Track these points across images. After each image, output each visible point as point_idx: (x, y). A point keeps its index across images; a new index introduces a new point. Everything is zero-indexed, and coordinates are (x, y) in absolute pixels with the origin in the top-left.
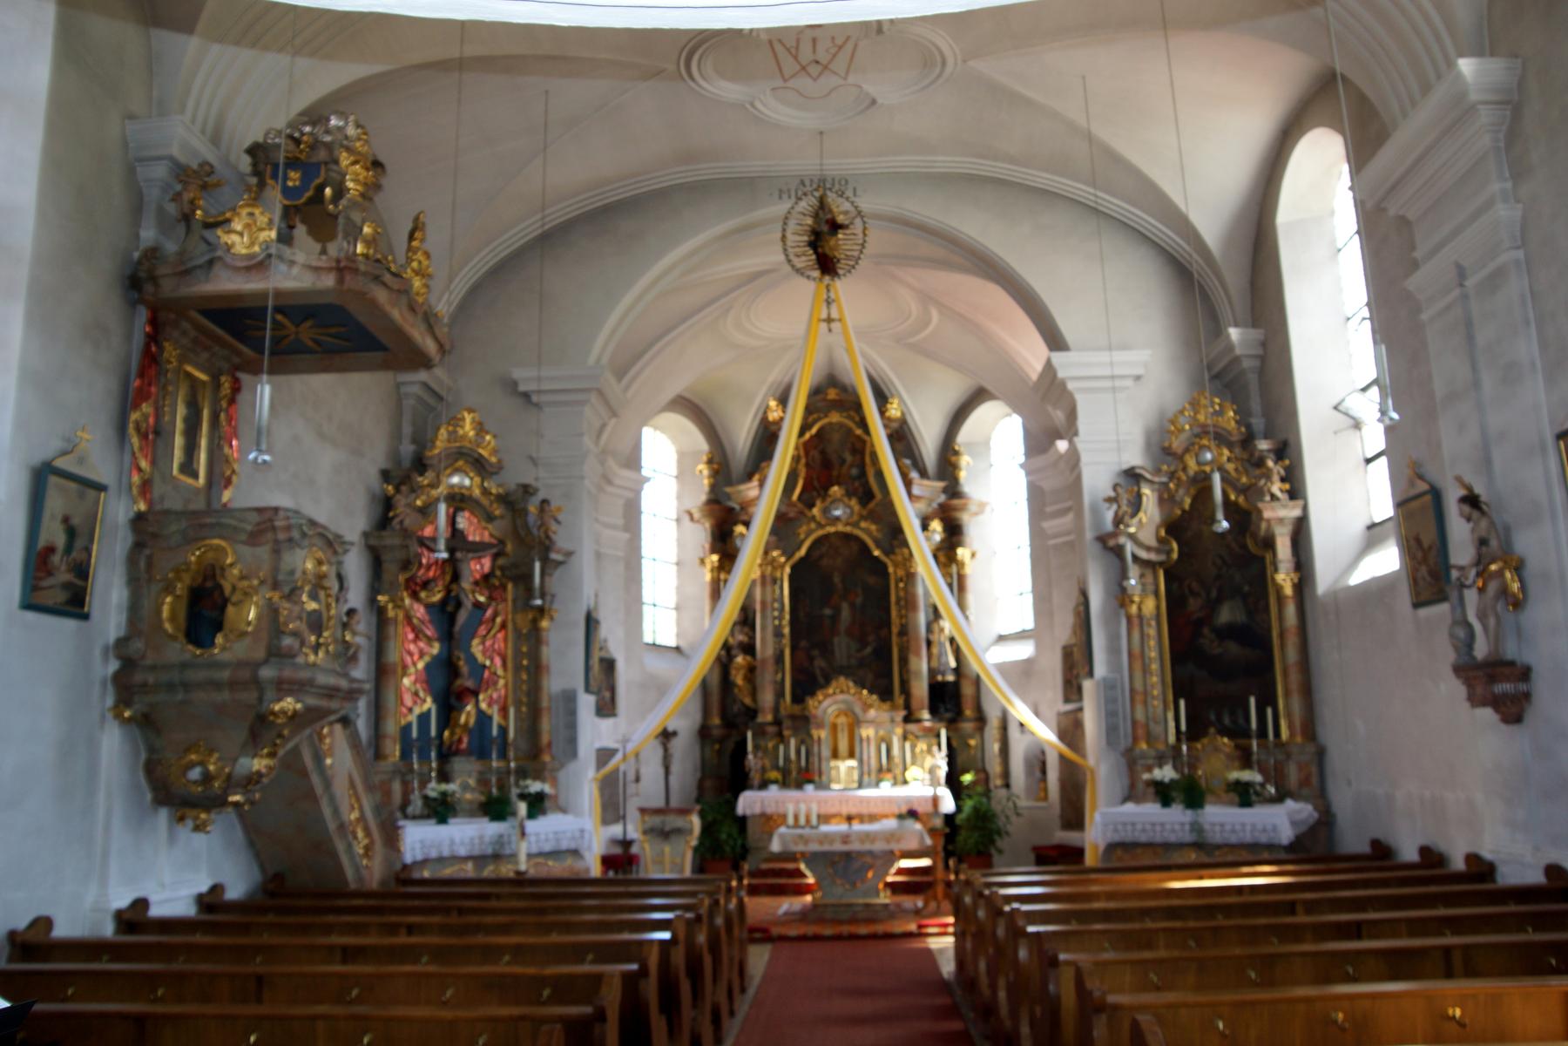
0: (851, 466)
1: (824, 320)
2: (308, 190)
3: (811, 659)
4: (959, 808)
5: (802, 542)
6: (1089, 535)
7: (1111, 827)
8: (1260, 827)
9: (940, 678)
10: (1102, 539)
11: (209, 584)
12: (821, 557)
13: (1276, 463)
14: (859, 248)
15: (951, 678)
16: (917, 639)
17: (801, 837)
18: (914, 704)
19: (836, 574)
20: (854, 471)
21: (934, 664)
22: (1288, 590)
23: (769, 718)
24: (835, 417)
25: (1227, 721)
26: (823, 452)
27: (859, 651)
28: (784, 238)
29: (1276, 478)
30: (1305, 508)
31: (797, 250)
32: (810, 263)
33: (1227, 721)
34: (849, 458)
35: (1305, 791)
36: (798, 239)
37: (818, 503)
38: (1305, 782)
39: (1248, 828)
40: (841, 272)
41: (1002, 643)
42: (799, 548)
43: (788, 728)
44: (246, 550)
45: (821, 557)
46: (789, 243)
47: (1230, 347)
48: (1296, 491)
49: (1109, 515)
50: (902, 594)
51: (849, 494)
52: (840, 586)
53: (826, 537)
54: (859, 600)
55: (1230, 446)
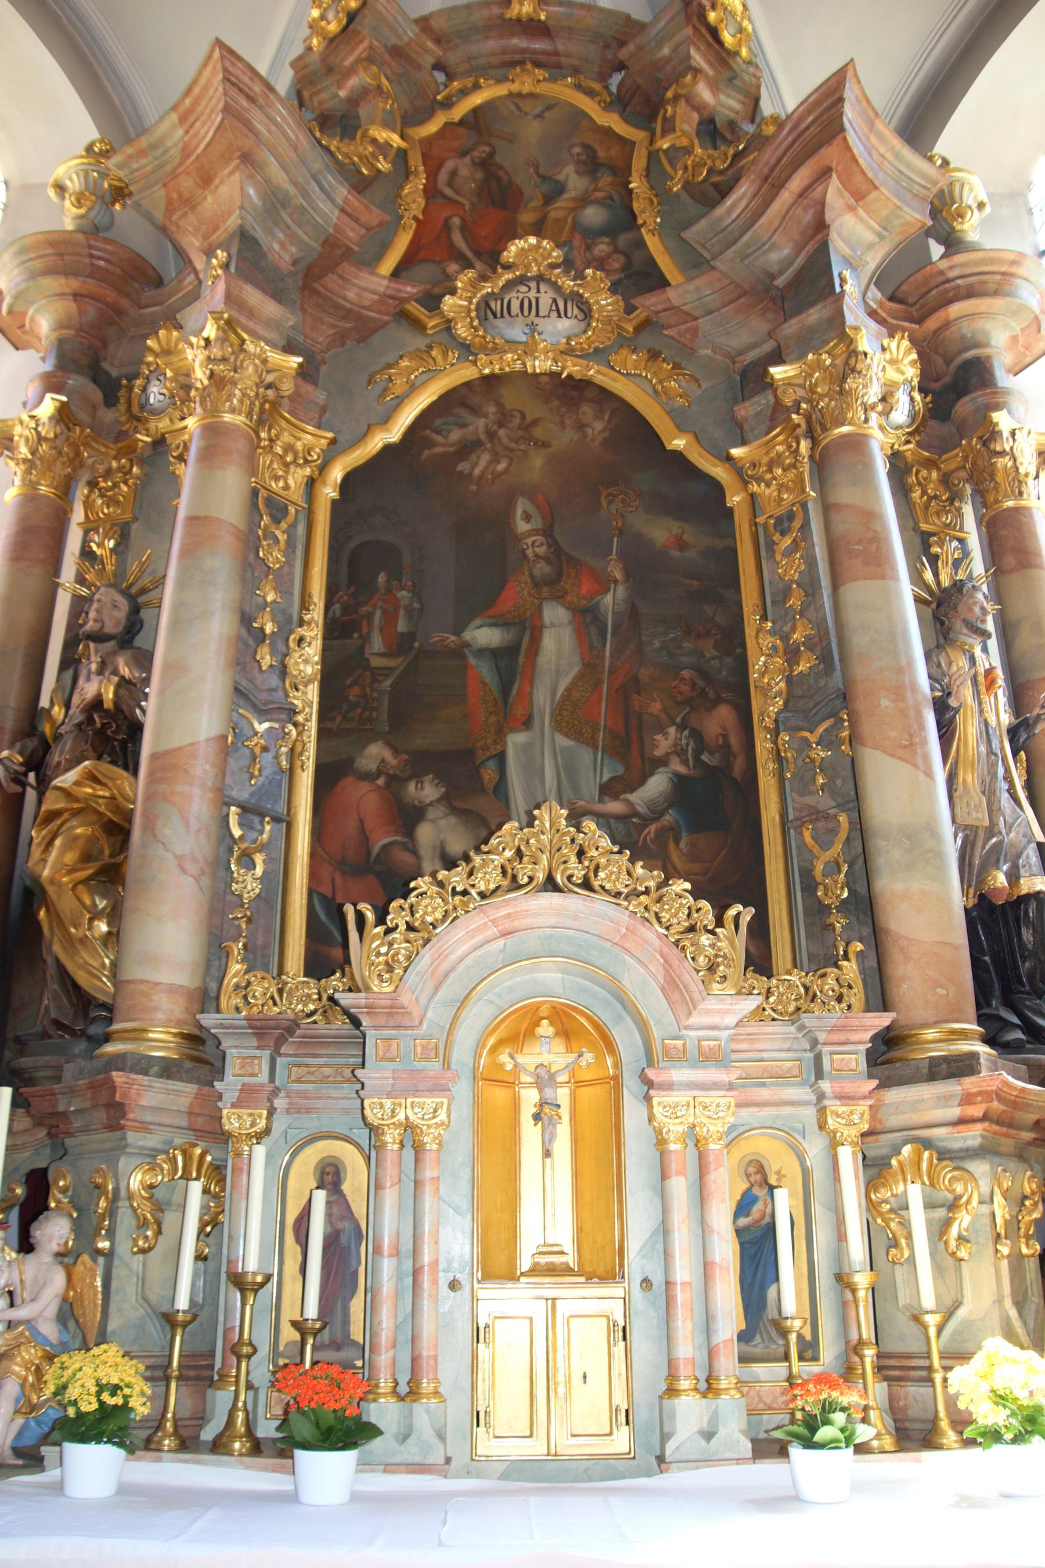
0: (584, 201)
5: (400, 402)
12: (467, 449)
19: (521, 506)
26: (485, 164)
27: (609, 790)
42: (386, 420)
45: (467, 449)
52: (535, 546)
53: (491, 381)
54: (611, 601)
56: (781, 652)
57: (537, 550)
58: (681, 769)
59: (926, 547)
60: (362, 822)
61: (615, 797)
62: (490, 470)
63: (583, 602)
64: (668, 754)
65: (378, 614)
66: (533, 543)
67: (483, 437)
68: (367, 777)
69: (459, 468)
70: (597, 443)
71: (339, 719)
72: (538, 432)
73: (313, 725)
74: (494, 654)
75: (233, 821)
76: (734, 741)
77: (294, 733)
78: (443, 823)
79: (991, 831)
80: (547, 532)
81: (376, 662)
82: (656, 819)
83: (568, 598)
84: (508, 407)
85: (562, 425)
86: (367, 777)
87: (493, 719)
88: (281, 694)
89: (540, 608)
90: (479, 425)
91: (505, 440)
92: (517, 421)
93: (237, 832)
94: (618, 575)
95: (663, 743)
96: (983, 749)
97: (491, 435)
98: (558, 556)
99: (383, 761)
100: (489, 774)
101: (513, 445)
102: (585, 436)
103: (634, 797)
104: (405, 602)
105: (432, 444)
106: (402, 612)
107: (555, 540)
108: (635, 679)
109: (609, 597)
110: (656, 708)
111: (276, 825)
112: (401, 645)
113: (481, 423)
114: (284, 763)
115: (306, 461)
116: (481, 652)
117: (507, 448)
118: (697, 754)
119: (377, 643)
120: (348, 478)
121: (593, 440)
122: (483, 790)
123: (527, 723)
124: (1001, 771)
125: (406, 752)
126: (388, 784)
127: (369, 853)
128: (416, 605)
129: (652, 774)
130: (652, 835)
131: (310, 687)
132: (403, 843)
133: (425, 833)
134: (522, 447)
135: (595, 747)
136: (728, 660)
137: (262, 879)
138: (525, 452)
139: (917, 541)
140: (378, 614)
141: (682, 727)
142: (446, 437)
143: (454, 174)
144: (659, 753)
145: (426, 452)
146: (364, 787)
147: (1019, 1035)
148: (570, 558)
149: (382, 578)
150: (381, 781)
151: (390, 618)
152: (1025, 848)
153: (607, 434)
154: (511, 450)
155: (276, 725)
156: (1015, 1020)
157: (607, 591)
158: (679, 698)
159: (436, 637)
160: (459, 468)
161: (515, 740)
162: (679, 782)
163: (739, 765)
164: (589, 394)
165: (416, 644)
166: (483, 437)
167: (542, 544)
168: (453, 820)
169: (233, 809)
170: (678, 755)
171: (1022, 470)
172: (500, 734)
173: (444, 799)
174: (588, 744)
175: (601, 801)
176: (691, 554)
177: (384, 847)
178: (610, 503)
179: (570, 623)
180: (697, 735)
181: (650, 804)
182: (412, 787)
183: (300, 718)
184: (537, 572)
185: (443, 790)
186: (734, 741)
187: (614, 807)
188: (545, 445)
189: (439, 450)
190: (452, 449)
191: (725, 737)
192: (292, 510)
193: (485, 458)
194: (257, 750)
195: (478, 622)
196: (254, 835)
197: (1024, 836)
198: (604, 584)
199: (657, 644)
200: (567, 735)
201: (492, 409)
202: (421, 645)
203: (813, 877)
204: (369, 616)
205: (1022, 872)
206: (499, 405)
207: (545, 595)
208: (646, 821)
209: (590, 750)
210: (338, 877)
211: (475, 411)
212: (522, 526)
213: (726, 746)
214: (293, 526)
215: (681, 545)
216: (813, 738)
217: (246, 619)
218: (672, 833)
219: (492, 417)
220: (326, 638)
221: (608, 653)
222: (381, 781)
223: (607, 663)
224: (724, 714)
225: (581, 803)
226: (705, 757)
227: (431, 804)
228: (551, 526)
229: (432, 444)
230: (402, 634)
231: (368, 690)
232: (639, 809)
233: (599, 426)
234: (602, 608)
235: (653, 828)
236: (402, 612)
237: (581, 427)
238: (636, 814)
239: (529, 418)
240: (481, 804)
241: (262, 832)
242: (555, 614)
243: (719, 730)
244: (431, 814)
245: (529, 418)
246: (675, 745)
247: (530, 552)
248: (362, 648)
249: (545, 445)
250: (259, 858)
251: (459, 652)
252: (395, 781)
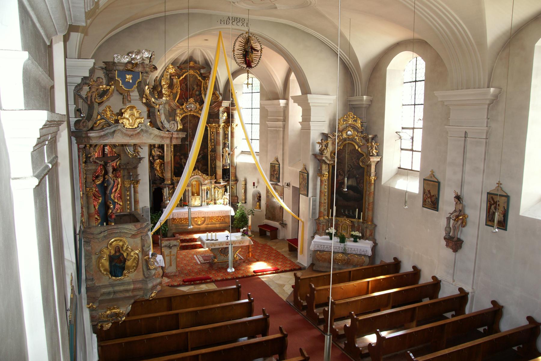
0: (196, 91)
1: (246, 84)
2: (135, 84)
3: (181, 159)
4: (236, 214)
6: (311, 153)
7: (317, 246)
8: (362, 250)
9: (225, 168)
10: (315, 155)
11: (118, 254)
13: (375, 144)
14: (259, 57)
15: (228, 167)
17: (213, 244)
18: (218, 177)
20: (197, 93)
22: (373, 182)
23: (169, 182)
24: (191, 72)
25: (347, 213)
28: (234, 51)
29: (374, 148)
30: (381, 159)
31: (238, 56)
32: (242, 61)
33: (347, 213)
34: (196, 88)
35: (371, 237)
36: (239, 53)
37: (185, 104)
38: (371, 235)
39: (359, 250)
40: (253, 66)
41: (243, 155)
44: (131, 240)
46: (236, 53)
47: (362, 100)
48: (380, 154)
49: (318, 148)
50: (213, 138)
51: (196, 101)
53: (187, 116)
55: (358, 132)
58: (202, 155)
72: (191, 121)
143: (183, 86)
162: (202, 156)
180: (204, 152)
188: (192, 123)
211: (186, 119)
224: (206, 150)
249: (192, 123)
252: (180, 156)
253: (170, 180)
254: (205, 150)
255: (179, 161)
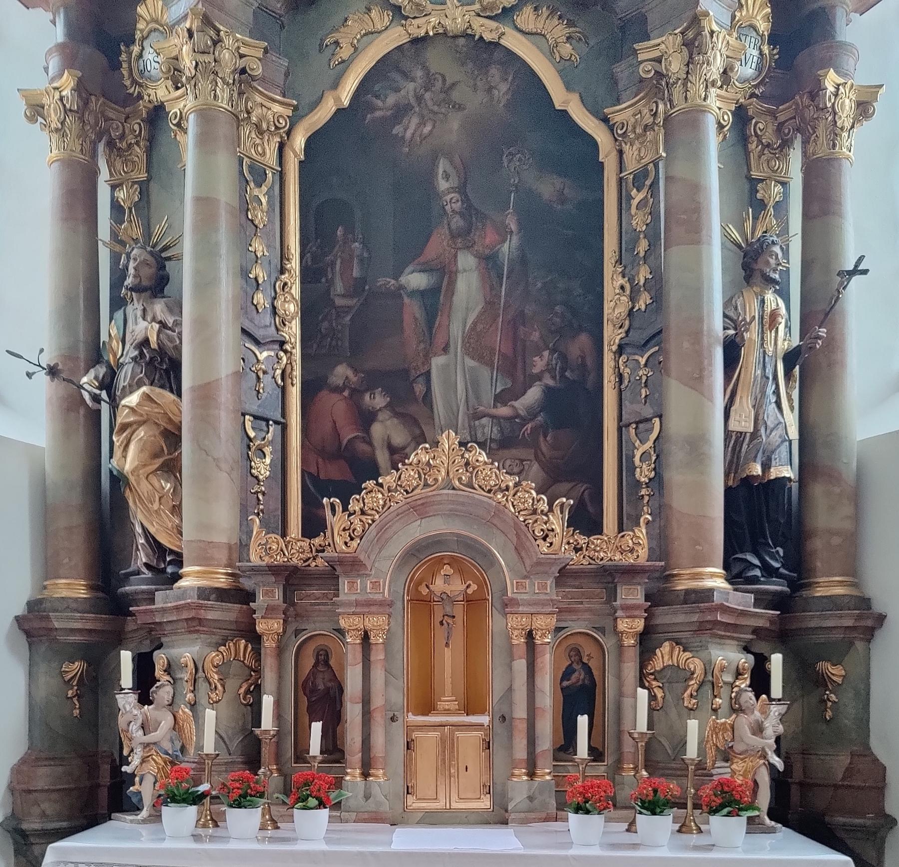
3: (366, 419)
5: (346, 64)
12: (401, 112)
16: (697, 335)
19: (442, 166)
21: (742, 422)
27: (501, 399)
43: (270, 611)
45: (401, 112)
52: (452, 202)
54: (508, 249)
56: (628, 292)
57: (453, 205)
58: (551, 383)
59: (754, 191)
60: (334, 422)
61: (505, 404)
62: (418, 133)
63: (487, 252)
64: (542, 372)
65: (338, 262)
66: (451, 199)
67: (413, 101)
68: (338, 390)
69: (394, 132)
70: (501, 105)
71: (315, 346)
72: (455, 95)
73: (297, 352)
74: (422, 294)
75: (248, 425)
76: (589, 362)
77: (285, 359)
78: (389, 423)
79: (755, 435)
80: (462, 189)
81: (339, 302)
82: (531, 420)
83: (476, 248)
84: (433, 71)
85: (475, 88)
86: (338, 390)
87: (422, 346)
88: (273, 328)
89: (456, 256)
90: (409, 88)
91: (430, 103)
92: (439, 84)
93: (252, 434)
94: (513, 227)
95: (539, 364)
96: (759, 372)
97: (419, 99)
98: (469, 211)
99: (347, 378)
100: (419, 388)
101: (436, 108)
102: (492, 98)
103: (517, 404)
104: (357, 252)
105: (373, 109)
106: (356, 261)
107: (466, 196)
108: (522, 314)
109: (506, 245)
110: (535, 336)
111: (276, 426)
112: (357, 287)
113: (411, 86)
114: (279, 382)
115: (277, 128)
116: (414, 293)
117: (432, 111)
118: (563, 370)
119: (339, 287)
120: (309, 142)
121: (499, 101)
122: (416, 400)
123: (445, 350)
124: (771, 388)
125: (363, 372)
126: (351, 395)
127: (340, 443)
128: (366, 255)
129: (531, 387)
130: (529, 432)
131: (294, 322)
132: (363, 438)
133: (377, 430)
134: (443, 110)
135: (492, 366)
136: (590, 297)
137: (270, 465)
138: (445, 115)
139: (747, 186)
140: (338, 262)
141: (553, 351)
142: (384, 101)
144: (536, 371)
145: (369, 116)
146: (335, 397)
147: (757, 572)
148: (478, 212)
149: (340, 232)
150: (346, 393)
151: (347, 265)
152: (779, 446)
153: (509, 97)
154: (436, 113)
155: (272, 354)
156: (756, 562)
157: (504, 241)
158: (553, 328)
159: (381, 281)
160: (394, 132)
161: (437, 362)
163: (591, 378)
164: (497, 55)
165: (367, 287)
166: (413, 101)
167: (458, 201)
168: (395, 421)
169: (247, 417)
170: (550, 372)
171: (839, 124)
172: (427, 359)
173: (389, 406)
174: (487, 365)
175: (495, 406)
176: (569, 206)
177: (349, 441)
178: (510, 161)
179: (476, 268)
180: (564, 357)
181: (529, 409)
182: (367, 397)
183: (288, 347)
184: (454, 226)
185: (388, 399)
186: (589, 362)
187: (504, 411)
189: (378, 114)
190: (389, 113)
191: (583, 358)
192: (270, 175)
193: (415, 121)
194: (261, 374)
195: (410, 268)
196: (264, 434)
197: (780, 437)
198: (504, 233)
199: (539, 285)
200: (473, 358)
201: (419, 73)
202: (370, 289)
203: (633, 462)
204: (333, 264)
205: (773, 463)
206: (425, 68)
207: (459, 245)
208: (525, 421)
209: (489, 369)
210: (320, 460)
211: (406, 75)
212: (443, 185)
213: (584, 365)
214: (271, 188)
215: (563, 201)
216: (643, 361)
217: (244, 273)
218: (543, 429)
219: (420, 81)
220: (302, 283)
221: (503, 293)
222: (346, 393)
223: (502, 301)
224: (584, 339)
225: (482, 408)
226: (566, 374)
227: (380, 410)
228: (465, 185)
229: (373, 109)
230: (356, 278)
231: (334, 324)
232: (520, 412)
233: (504, 87)
234: (500, 255)
235: (529, 426)
236: (356, 261)
237: (490, 90)
238: (518, 416)
239: (449, 82)
240: (413, 409)
241: (268, 432)
242: (466, 261)
243: (578, 353)
244: (381, 416)
245: (449, 82)
246: (548, 365)
247: (448, 208)
248: (328, 292)
249: (460, 107)
250: (268, 450)
251: (397, 294)
252: (356, 393)
253: (223, 556)
254: (580, 344)
255: (348, 434)
